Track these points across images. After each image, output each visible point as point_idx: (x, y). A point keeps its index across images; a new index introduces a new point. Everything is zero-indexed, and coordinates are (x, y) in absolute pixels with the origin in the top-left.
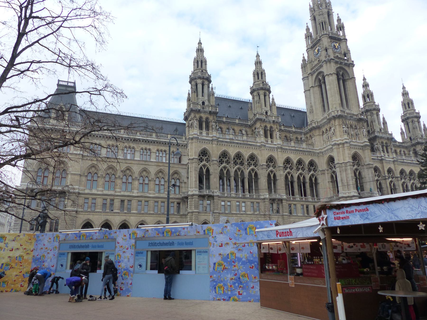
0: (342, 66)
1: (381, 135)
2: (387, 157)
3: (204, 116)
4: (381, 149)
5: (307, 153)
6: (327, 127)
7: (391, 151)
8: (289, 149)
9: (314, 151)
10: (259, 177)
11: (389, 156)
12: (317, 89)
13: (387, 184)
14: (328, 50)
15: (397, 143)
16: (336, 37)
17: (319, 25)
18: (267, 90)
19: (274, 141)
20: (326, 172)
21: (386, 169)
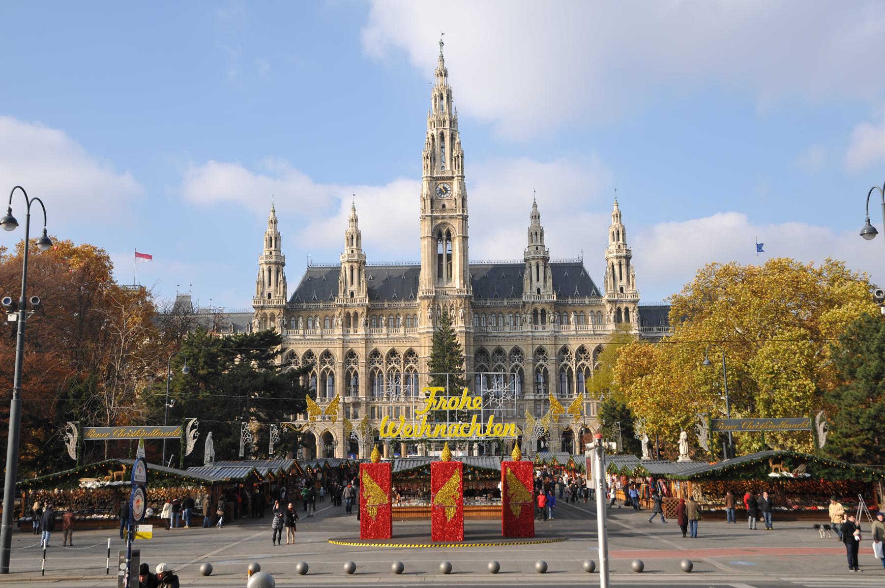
3: (268, 312)
5: (404, 340)
8: (378, 339)
11: (544, 328)
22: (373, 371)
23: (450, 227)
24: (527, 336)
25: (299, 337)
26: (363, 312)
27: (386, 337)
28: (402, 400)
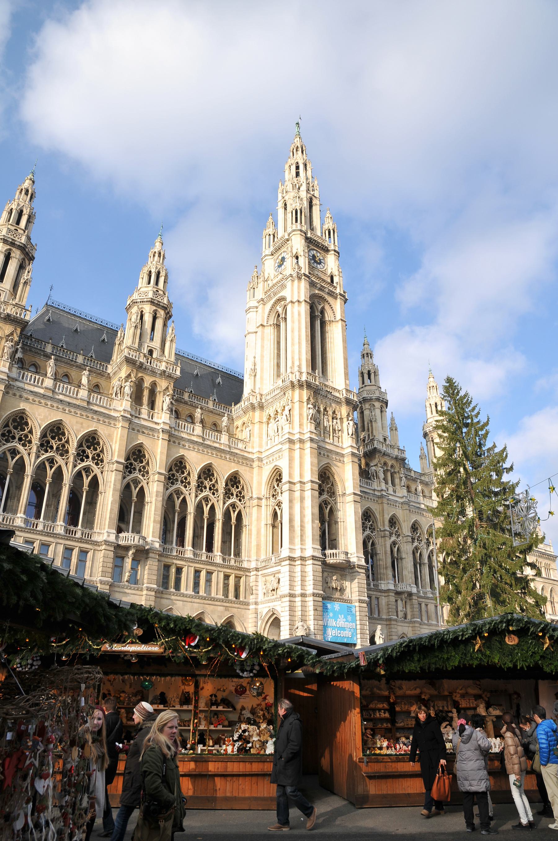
0: (323, 294)
1: (384, 449)
2: (392, 493)
4: (382, 476)
5: (228, 457)
6: (278, 406)
7: (400, 484)
9: (246, 454)
10: (101, 488)
12: (270, 332)
13: (385, 547)
14: (299, 257)
15: (412, 472)
16: (318, 243)
17: (291, 214)
18: (163, 306)
19: (155, 415)
20: (264, 502)
21: (387, 517)
22: (170, 496)
23: (327, 307)
24: (382, 497)
25: (42, 391)
26: (167, 388)
27: (201, 441)
28: (218, 560)
